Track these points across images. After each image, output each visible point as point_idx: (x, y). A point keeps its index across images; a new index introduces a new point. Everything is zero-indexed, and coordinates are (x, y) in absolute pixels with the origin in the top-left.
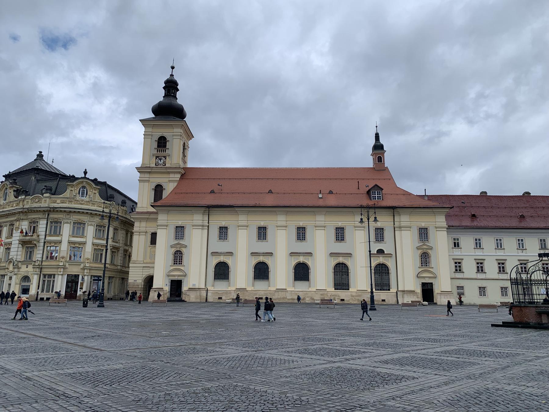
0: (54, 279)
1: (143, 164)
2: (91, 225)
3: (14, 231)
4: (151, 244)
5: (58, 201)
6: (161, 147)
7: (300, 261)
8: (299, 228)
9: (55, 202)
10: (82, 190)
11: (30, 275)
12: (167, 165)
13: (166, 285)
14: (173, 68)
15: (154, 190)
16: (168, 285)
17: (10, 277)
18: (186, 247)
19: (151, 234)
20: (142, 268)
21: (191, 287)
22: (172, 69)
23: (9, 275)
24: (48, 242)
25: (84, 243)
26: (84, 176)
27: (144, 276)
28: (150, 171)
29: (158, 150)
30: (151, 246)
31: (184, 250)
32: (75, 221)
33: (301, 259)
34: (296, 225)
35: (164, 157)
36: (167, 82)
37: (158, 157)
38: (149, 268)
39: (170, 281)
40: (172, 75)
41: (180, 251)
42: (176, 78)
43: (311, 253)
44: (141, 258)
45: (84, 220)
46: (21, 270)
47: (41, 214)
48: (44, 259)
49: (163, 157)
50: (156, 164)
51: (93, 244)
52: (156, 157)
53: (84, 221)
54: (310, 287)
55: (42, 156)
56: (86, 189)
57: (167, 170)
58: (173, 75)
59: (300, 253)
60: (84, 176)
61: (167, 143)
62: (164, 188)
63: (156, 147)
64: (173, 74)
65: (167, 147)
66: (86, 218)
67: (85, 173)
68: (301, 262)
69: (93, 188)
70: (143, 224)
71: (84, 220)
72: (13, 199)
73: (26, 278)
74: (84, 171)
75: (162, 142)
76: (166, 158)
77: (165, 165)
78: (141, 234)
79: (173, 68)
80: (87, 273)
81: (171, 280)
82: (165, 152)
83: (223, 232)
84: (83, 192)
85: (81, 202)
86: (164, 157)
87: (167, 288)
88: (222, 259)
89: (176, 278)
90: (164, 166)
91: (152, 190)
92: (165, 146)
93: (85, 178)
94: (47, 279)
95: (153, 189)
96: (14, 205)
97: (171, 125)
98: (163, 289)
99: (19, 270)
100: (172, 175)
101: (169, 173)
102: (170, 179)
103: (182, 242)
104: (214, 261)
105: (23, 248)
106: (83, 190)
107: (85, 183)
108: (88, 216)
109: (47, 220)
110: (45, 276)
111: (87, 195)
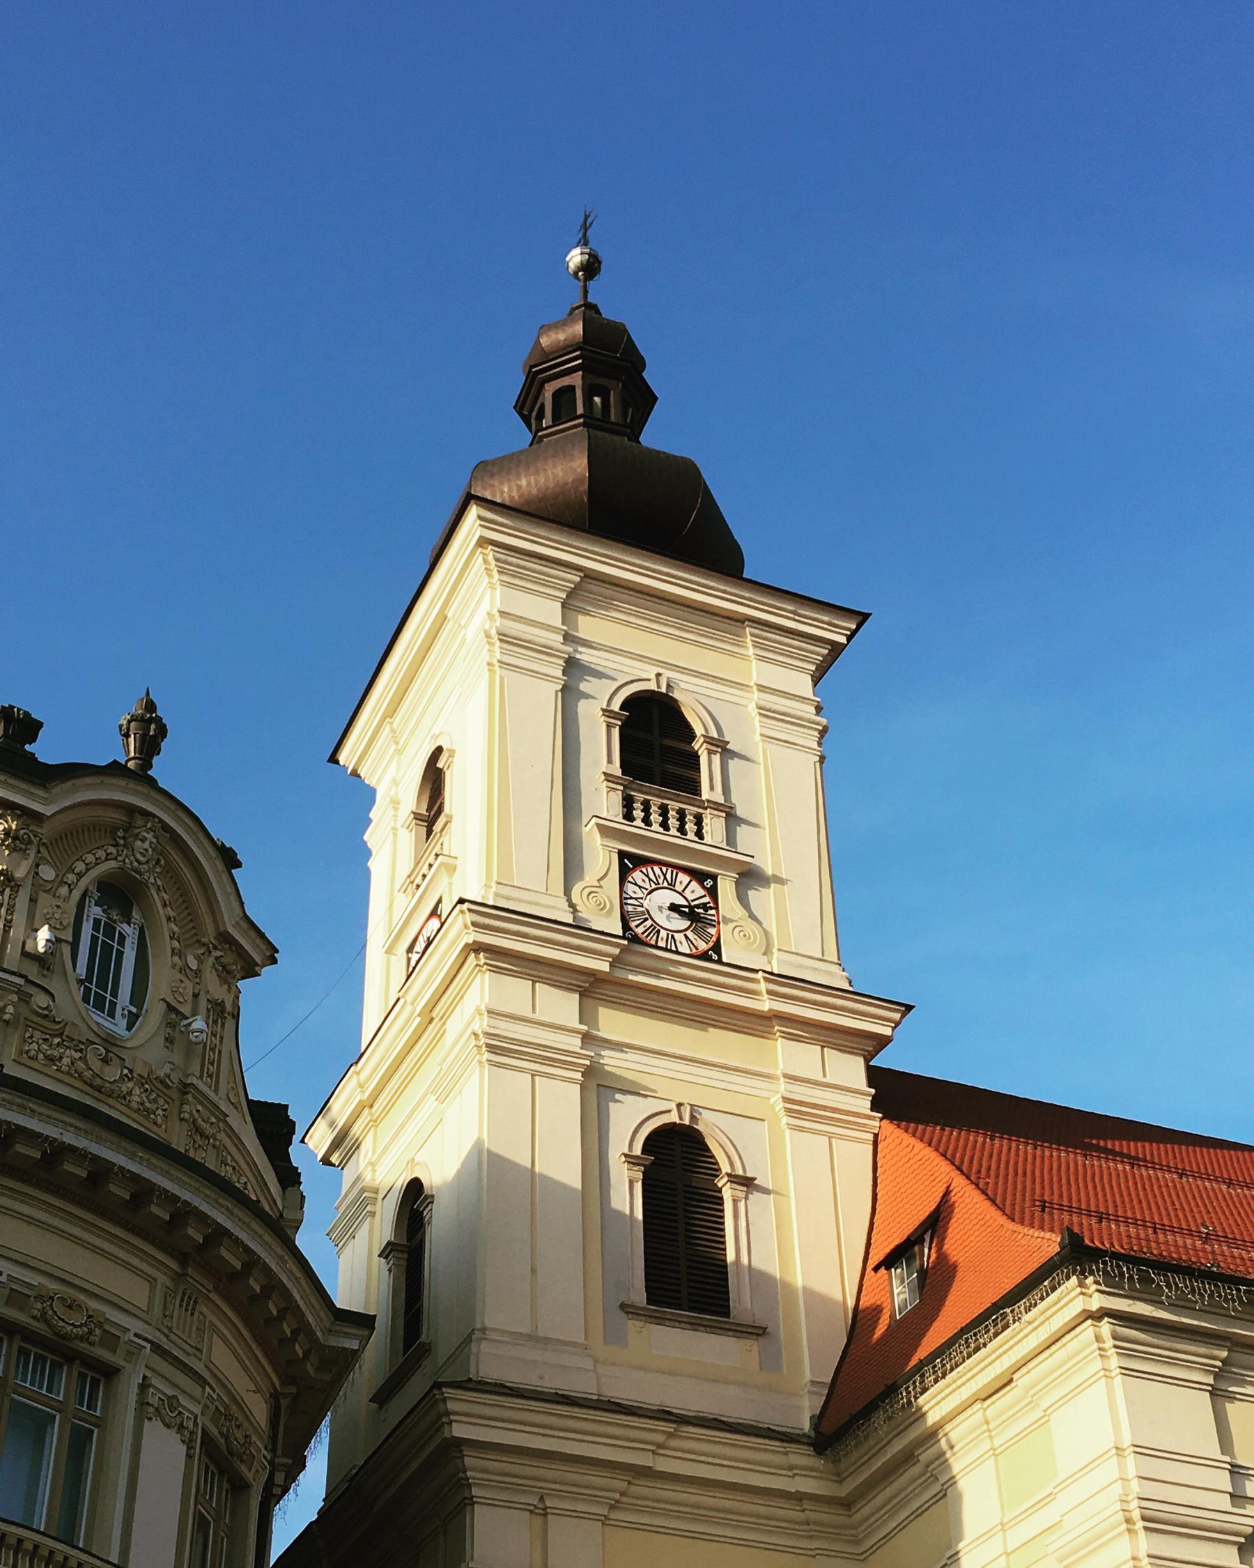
1: (505, 891)
2: (169, 1412)
10: (97, 922)
28: (604, 966)
29: (628, 803)
37: (640, 861)
45: (94, 1305)
49: (683, 878)
52: (622, 855)
53: (111, 1341)
56: (136, 914)
63: (616, 770)
65: (706, 794)
66: (135, 1291)
69: (210, 936)
76: (713, 892)
77: (717, 948)
82: (699, 834)
84: (107, 948)
85: (96, 1065)
90: (704, 956)
106: (110, 930)
107: (145, 843)
108: (152, 1281)
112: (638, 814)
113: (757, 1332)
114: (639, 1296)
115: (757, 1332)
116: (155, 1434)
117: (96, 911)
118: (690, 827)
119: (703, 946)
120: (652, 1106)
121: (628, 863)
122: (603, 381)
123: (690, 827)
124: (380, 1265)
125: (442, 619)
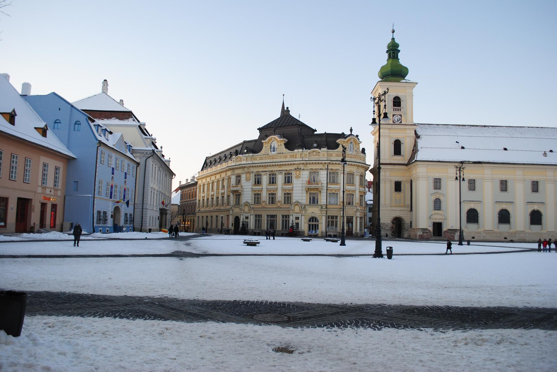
0: (336, 220)
3: (294, 180)
4: (395, 191)
5: (334, 155)
6: (396, 106)
7: (534, 209)
8: (533, 182)
9: (331, 155)
11: (316, 216)
12: (403, 123)
13: (430, 226)
14: (393, 32)
15: (393, 144)
16: (431, 226)
17: (296, 217)
18: (444, 195)
19: (395, 183)
20: (390, 211)
21: (450, 228)
22: (392, 33)
23: (294, 216)
24: (329, 189)
25: (354, 191)
26: (350, 133)
27: (392, 217)
28: (390, 127)
29: (394, 109)
30: (396, 192)
31: (442, 198)
32: (348, 172)
33: (536, 207)
34: (531, 180)
35: (400, 115)
36: (389, 47)
37: (394, 115)
38: (395, 211)
39: (433, 223)
40: (393, 39)
41: (439, 199)
42: (397, 41)
43: (543, 203)
44: (388, 202)
46: (307, 212)
47: (321, 165)
48: (328, 203)
50: (393, 121)
51: (360, 191)
53: (354, 172)
54: (542, 229)
55: (289, 111)
57: (405, 127)
58: (394, 39)
59: (535, 203)
60: (350, 133)
61: (402, 103)
62: (402, 142)
64: (394, 37)
66: (355, 169)
67: (351, 130)
68: (536, 210)
70: (388, 174)
71: (353, 171)
72: (285, 151)
73: (313, 219)
74: (350, 129)
75: (397, 102)
76: (401, 116)
77: (401, 122)
78: (386, 182)
79: (393, 32)
80: (359, 215)
81: (433, 223)
82: (400, 111)
83: (472, 185)
86: (400, 115)
87: (431, 229)
88: (472, 206)
89: (438, 221)
90: (400, 123)
91: (392, 144)
92: (400, 106)
93: (351, 135)
94: (330, 220)
95: (393, 143)
96: (288, 157)
97: (405, 86)
98: (427, 229)
99: (306, 212)
100: (408, 131)
101: (406, 129)
102: (407, 135)
103: (439, 191)
104: (466, 208)
105: (307, 194)
107: (352, 139)
109: (327, 171)
110: (329, 216)
111: (353, 150)
112: (395, 110)
113: (403, 156)
114: (393, 154)
115: (403, 156)
116: (357, 176)
117: (350, 145)
118: (399, 110)
119: (400, 122)
120: (394, 138)
121: (393, 115)
122: (394, 52)
123: (399, 110)
124: (376, 148)
125: (377, 89)
